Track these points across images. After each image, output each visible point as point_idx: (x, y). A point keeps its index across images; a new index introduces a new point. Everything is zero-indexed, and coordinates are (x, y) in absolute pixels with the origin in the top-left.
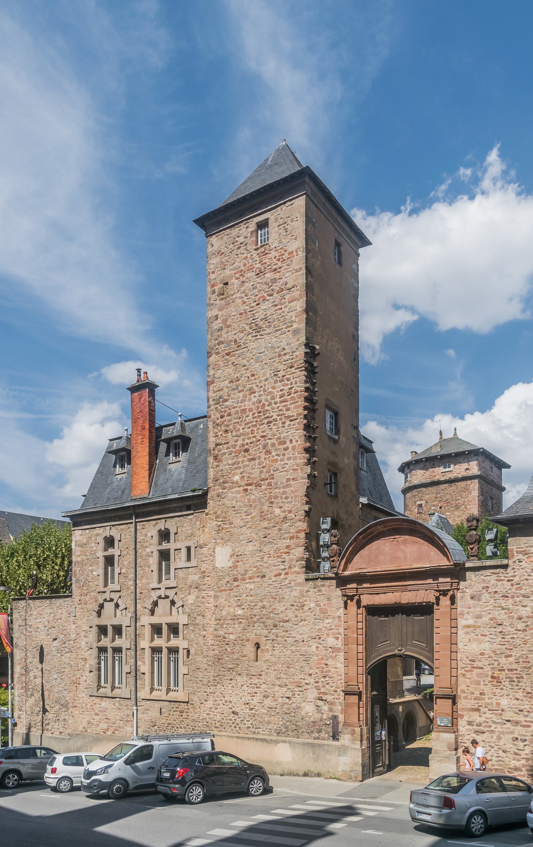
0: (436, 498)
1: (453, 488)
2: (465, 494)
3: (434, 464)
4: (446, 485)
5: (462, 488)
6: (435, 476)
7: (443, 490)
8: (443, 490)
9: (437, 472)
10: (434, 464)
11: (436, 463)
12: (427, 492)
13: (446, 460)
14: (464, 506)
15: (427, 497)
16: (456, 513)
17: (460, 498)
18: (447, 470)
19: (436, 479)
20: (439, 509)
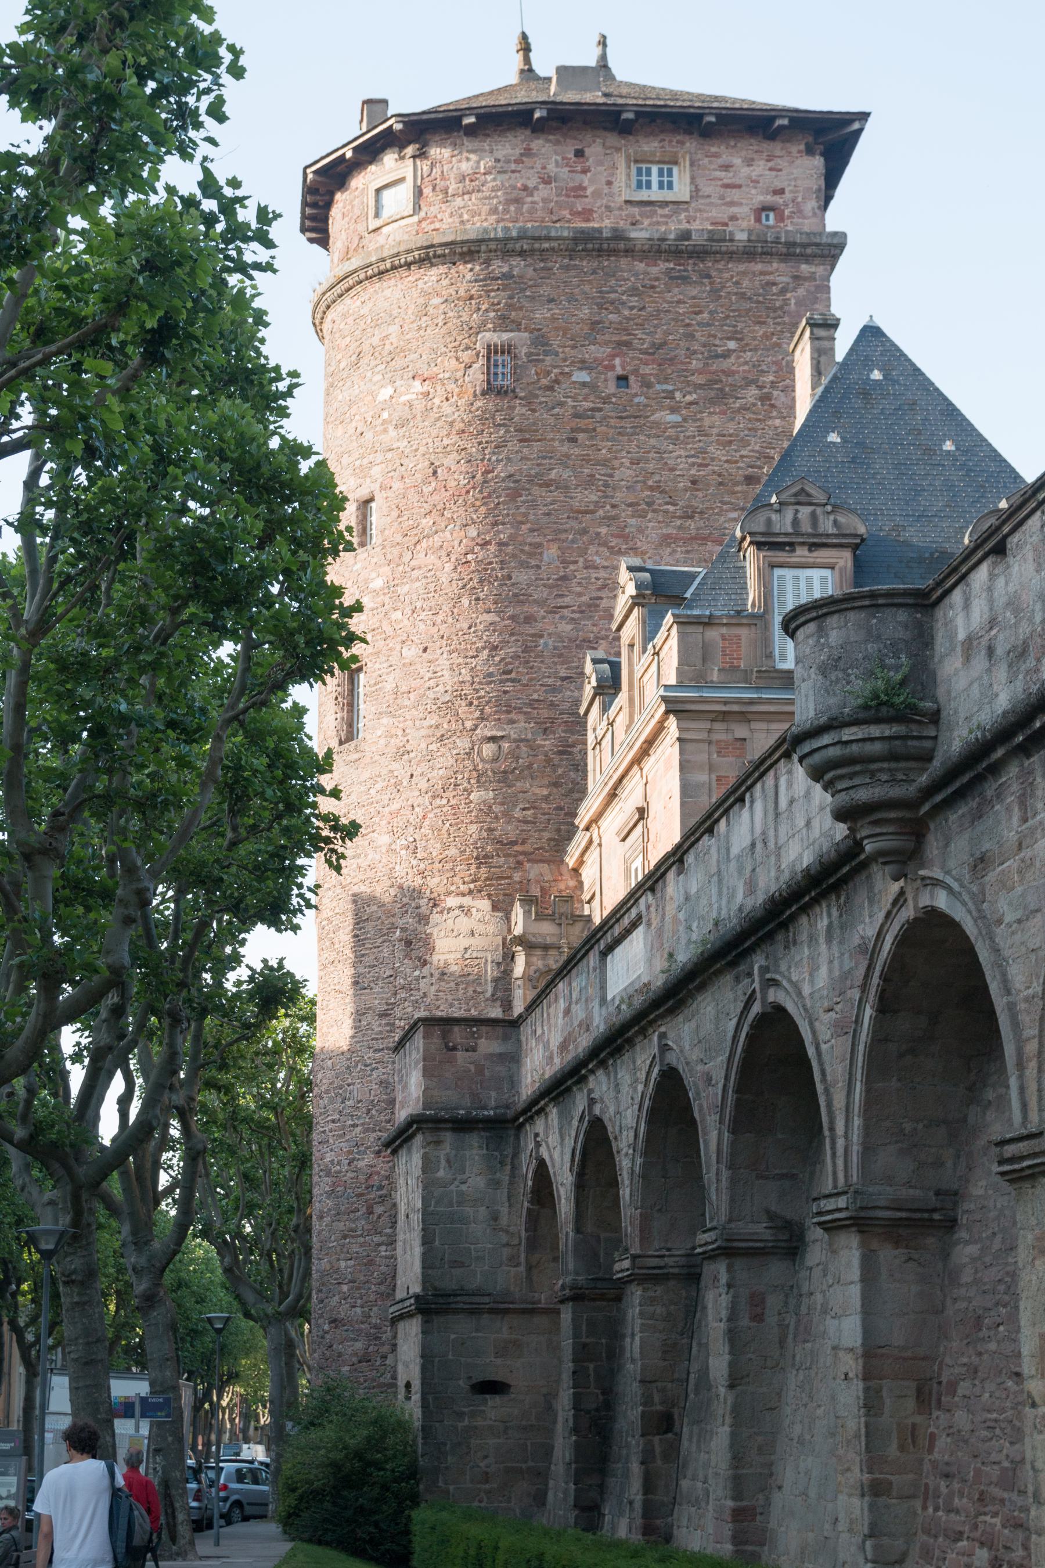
0: (595, 325)
1: (694, 292)
2: (760, 331)
3: (579, 153)
4: (654, 270)
5: (742, 296)
6: (587, 214)
7: (634, 292)
8: (634, 292)
9: (597, 194)
10: (579, 153)
11: (594, 150)
12: (545, 290)
13: (650, 146)
14: (753, 392)
15: (541, 314)
16: (713, 420)
17: (732, 345)
18: (655, 194)
19: (604, 223)
20: (611, 388)
